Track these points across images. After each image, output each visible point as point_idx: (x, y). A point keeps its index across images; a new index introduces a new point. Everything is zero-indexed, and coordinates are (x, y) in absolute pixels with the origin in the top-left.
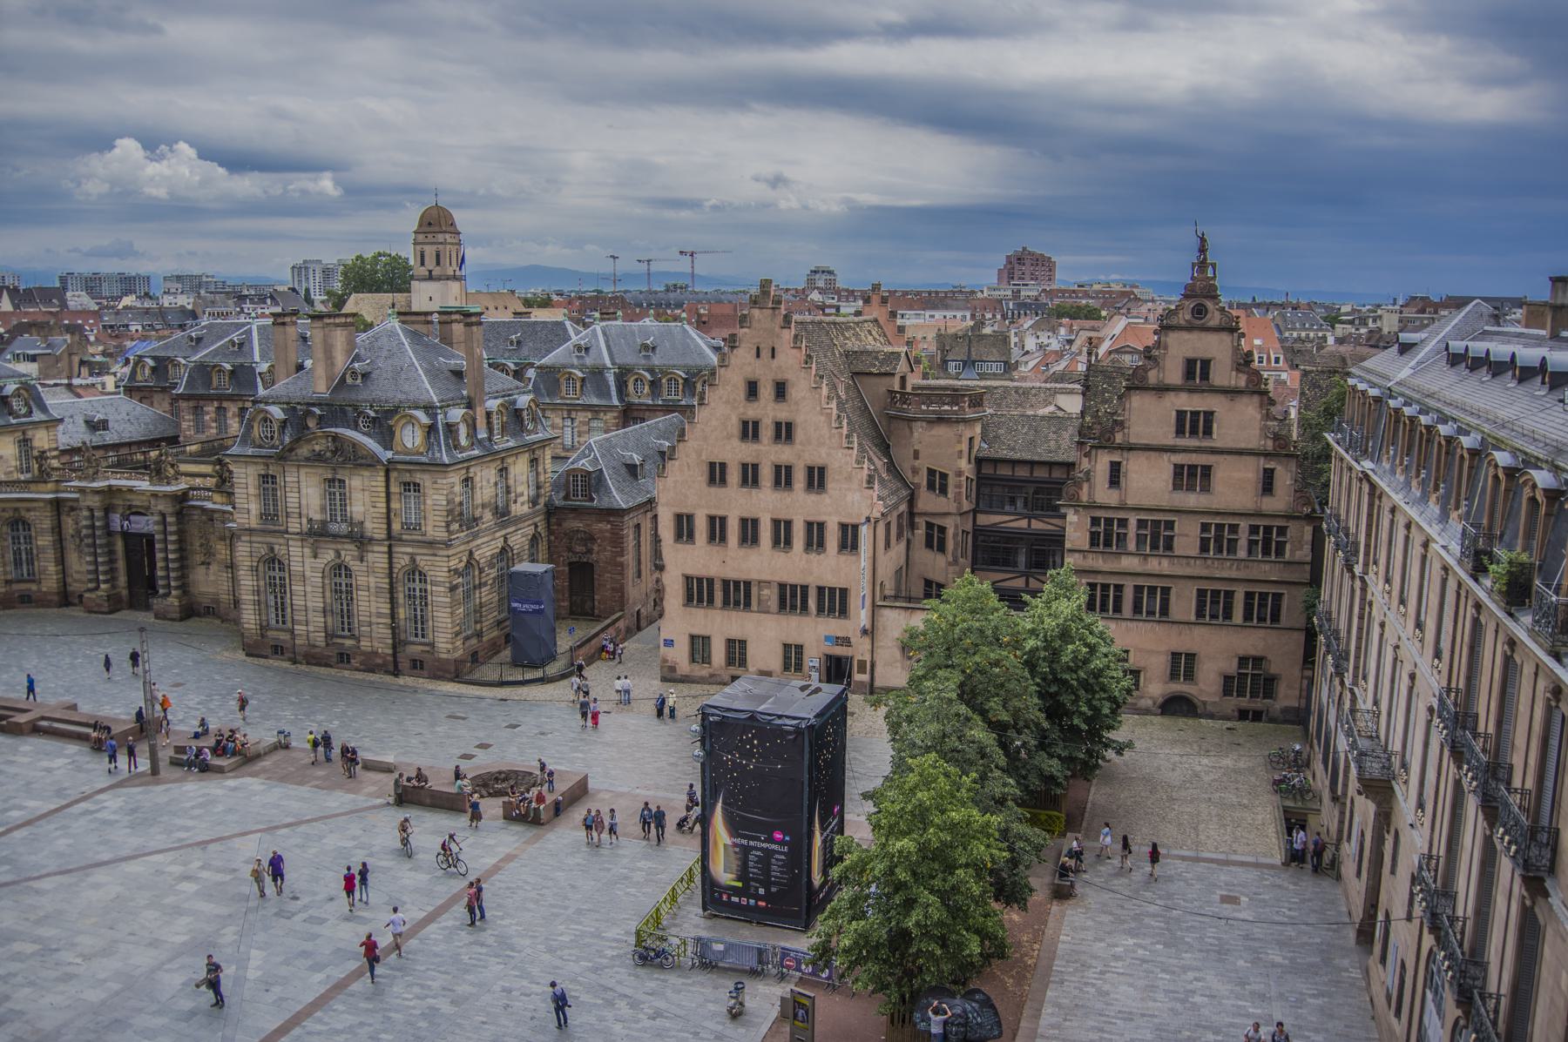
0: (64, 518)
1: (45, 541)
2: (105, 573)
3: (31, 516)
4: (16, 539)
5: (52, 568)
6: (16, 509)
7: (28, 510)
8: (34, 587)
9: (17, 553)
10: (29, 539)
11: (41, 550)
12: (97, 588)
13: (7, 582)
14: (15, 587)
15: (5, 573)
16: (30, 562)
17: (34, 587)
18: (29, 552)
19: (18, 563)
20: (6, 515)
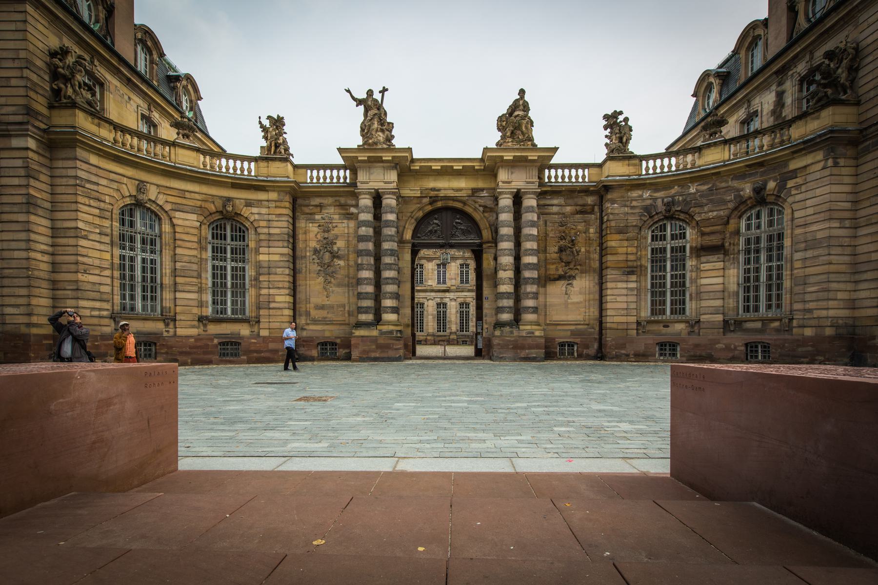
0: (301, 224)
1: (274, 254)
2: (397, 296)
3: (252, 213)
4: (218, 252)
5: (282, 298)
6: (229, 199)
7: (249, 204)
8: (244, 330)
9: (218, 273)
10: (240, 254)
11: (269, 268)
12: (378, 320)
13: (201, 319)
14: (213, 329)
15: (201, 304)
16: (239, 289)
17: (244, 330)
18: (239, 275)
19: (218, 290)
20: (212, 208)
